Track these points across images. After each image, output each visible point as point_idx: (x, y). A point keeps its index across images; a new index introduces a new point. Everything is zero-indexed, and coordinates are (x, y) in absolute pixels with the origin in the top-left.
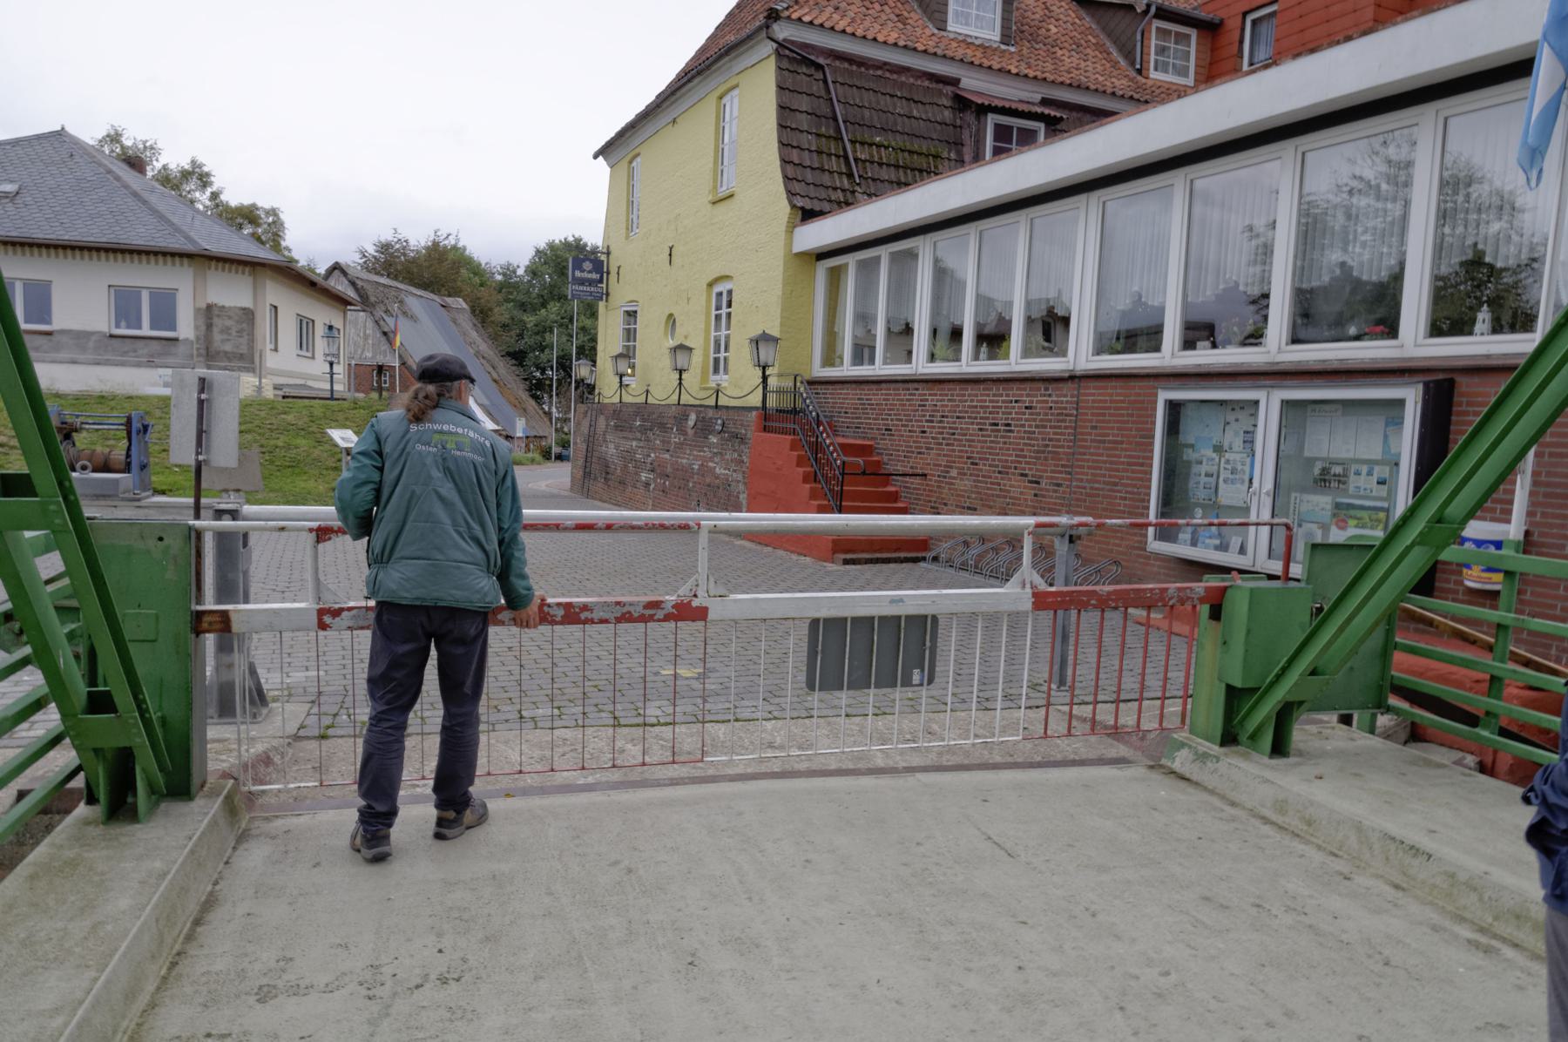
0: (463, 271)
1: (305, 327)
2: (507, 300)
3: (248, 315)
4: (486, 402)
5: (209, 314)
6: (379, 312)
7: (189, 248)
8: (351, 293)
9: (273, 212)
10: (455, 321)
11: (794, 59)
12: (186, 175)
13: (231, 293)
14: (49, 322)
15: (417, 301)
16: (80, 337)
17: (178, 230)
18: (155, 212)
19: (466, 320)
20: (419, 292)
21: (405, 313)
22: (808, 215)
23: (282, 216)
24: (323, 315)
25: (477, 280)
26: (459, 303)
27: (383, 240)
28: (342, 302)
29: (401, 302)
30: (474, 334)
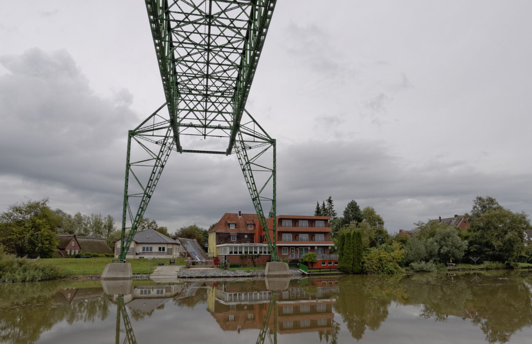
0: (196, 231)
1: (176, 248)
2: (204, 236)
3: (172, 249)
4: (199, 257)
5: (168, 249)
6: (183, 244)
7: (166, 242)
8: (179, 243)
9: (166, 228)
10: (194, 244)
11: (217, 233)
12: (152, 223)
13: (170, 247)
14: (152, 251)
15: (189, 241)
16: (155, 253)
17: (165, 240)
18: (163, 238)
19: (196, 243)
20: (189, 240)
21: (187, 244)
22: (217, 244)
23: (167, 228)
24: (177, 247)
25: (199, 232)
26: (195, 240)
27: (182, 227)
28: (179, 245)
29: (186, 242)
30: (197, 245)
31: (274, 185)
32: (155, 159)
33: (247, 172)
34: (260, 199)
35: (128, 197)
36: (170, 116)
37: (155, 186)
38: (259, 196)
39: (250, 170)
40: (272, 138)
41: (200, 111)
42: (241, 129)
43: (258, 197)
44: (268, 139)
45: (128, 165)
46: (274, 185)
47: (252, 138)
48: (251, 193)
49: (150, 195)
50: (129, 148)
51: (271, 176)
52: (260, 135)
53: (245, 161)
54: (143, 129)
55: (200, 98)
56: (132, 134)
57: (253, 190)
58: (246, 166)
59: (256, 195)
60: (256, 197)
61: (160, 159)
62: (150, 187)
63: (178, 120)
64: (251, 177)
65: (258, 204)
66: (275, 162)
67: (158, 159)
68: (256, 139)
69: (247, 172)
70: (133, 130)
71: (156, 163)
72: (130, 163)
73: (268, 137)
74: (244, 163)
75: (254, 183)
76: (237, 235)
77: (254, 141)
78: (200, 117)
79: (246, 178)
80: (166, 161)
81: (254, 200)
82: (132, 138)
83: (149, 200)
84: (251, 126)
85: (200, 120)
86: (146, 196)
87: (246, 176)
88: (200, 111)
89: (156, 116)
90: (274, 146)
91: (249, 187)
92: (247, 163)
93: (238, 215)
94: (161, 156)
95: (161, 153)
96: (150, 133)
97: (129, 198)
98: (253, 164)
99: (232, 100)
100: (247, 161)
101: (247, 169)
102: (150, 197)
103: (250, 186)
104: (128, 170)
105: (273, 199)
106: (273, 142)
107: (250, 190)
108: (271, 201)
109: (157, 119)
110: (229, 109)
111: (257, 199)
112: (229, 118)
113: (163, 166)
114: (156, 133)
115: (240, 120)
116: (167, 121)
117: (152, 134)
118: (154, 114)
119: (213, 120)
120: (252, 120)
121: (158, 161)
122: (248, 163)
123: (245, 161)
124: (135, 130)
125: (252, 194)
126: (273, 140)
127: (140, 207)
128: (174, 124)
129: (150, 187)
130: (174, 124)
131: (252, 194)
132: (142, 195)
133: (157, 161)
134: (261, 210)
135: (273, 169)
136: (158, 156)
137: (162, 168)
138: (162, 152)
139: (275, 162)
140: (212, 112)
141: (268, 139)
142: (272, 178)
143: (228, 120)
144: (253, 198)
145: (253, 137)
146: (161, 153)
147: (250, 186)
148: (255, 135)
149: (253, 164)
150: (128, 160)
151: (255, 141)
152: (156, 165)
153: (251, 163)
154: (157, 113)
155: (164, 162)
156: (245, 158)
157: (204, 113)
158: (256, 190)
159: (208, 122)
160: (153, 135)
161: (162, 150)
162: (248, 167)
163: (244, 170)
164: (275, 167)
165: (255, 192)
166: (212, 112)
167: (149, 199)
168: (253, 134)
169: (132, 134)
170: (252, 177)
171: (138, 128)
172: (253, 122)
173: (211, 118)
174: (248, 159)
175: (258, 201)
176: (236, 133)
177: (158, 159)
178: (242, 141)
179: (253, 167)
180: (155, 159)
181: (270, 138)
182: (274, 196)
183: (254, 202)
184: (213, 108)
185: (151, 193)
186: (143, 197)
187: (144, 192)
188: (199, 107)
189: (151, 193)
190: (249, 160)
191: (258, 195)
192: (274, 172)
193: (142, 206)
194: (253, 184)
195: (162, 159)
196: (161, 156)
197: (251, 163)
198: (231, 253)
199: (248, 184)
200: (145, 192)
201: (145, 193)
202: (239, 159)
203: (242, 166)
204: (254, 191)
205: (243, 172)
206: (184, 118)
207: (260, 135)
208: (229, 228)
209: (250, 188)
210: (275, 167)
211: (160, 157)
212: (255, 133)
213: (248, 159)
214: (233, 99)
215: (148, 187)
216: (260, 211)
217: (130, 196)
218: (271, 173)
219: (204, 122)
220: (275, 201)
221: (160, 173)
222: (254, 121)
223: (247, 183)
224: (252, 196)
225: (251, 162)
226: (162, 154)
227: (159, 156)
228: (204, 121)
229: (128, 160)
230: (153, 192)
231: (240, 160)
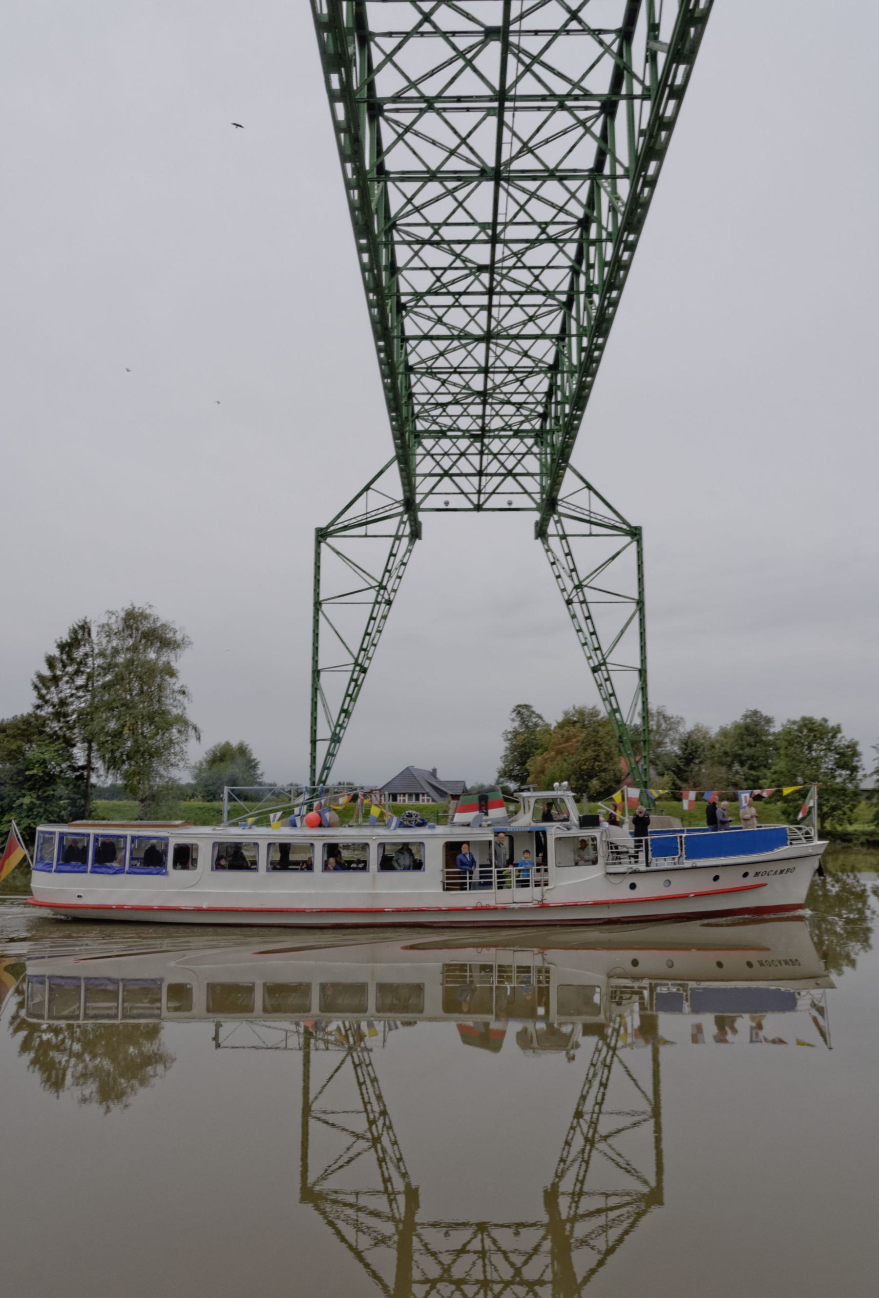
31: (642, 634)
32: (372, 587)
33: (576, 607)
34: (610, 667)
36: (405, 491)
37: (375, 645)
38: (608, 660)
39: (584, 602)
40: (634, 524)
41: (466, 475)
42: (560, 509)
43: (604, 664)
44: (624, 527)
45: (318, 604)
46: (642, 634)
47: (585, 528)
48: (589, 655)
49: (366, 666)
50: (317, 568)
52: (606, 520)
53: (573, 580)
54: (346, 524)
55: (463, 443)
56: (322, 535)
57: (592, 648)
58: (574, 593)
59: (600, 657)
60: (600, 665)
61: (385, 588)
62: (365, 650)
63: (418, 499)
64: (587, 618)
65: (606, 680)
66: (641, 580)
67: (381, 587)
68: (596, 530)
69: (576, 607)
70: (324, 525)
71: (377, 597)
72: (321, 598)
73: (624, 522)
74: (570, 586)
75: (594, 633)
77: (591, 535)
78: (467, 488)
79: (575, 620)
80: (395, 591)
81: (595, 670)
82: (323, 545)
83: (364, 678)
84: (583, 499)
85: (465, 494)
86: (358, 668)
87: (574, 617)
88: (466, 475)
89: (370, 491)
90: (639, 542)
91: (583, 641)
92: (576, 587)
94: (388, 581)
95: (387, 574)
96: (361, 531)
97: (322, 674)
98: (591, 588)
99: (536, 443)
101: (576, 599)
102: (364, 670)
103: (586, 639)
104: (318, 615)
105: (639, 666)
106: (635, 533)
107: (585, 647)
108: (636, 673)
109: (373, 502)
110: (532, 464)
111: (603, 668)
112: (533, 485)
113: (389, 603)
114: (372, 529)
115: (558, 490)
116: (397, 502)
117: (364, 534)
118: (367, 488)
119: (493, 493)
120: (584, 485)
121: (382, 592)
122: (579, 587)
123: (573, 580)
124: (328, 527)
125: (590, 658)
126: (636, 528)
127: (347, 695)
128: (410, 505)
129: (365, 650)
130: (410, 505)
131: (590, 658)
132: (351, 667)
133: (378, 591)
134: (613, 695)
135: (636, 597)
136: (380, 580)
137: (388, 607)
138: (389, 571)
139: (641, 580)
140: (492, 475)
141: (624, 527)
142: (636, 619)
143: (529, 490)
144: (592, 665)
145: (588, 525)
146: (387, 574)
147: (586, 639)
148: (592, 520)
149: (591, 588)
150: (317, 594)
151: (594, 533)
152: (377, 602)
153: (586, 586)
154: (372, 486)
155: (393, 594)
156: (571, 576)
157: (477, 478)
158: (599, 648)
159: (483, 498)
160: (366, 536)
161: (389, 568)
162: (580, 594)
163: (569, 602)
164: (641, 593)
165: (598, 652)
166: (492, 475)
167: (362, 675)
168: (588, 518)
170: (589, 618)
171: (332, 524)
172: (586, 490)
173: (489, 489)
174: (578, 576)
175: (605, 673)
176: (549, 520)
177: (381, 587)
178: (564, 537)
179: (590, 594)
180: (373, 587)
181: (629, 525)
182: (642, 661)
183: (596, 674)
184: (494, 467)
185: (368, 661)
186: (353, 671)
187: (353, 661)
188: (464, 466)
190: (581, 579)
191: (604, 659)
192: (640, 603)
193: (350, 692)
194: (592, 634)
195: (389, 588)
196: (388, 581)
197: (586, 586)
199: (580, 633)
200: (357, 660)
201: (356, 664)
202: (558, 577)
203: (565, 593)
204: (595, 649)
205: (569, 609)
206: (431, 492)
207: (606, 520)
209: (585, 644)
210: (641, 593)
211: (384, 584)
212: (592, 515)
213: (578, 576)
214: (539, 440)
215: (362, 649)
216: (611, 695)
217: (324, 669)
218: (633, 607)
219: (474, 498)
220: (645, 671)
221: (384, 617)
222: (589, 487)
223: (578, 631)
224: (591, 661)
225: (584, 583)
226: (390, 577)
227: (382, 580)
228: (476, 496)
229: (317, 594)
230: (370, 659)
231: (559, 580)
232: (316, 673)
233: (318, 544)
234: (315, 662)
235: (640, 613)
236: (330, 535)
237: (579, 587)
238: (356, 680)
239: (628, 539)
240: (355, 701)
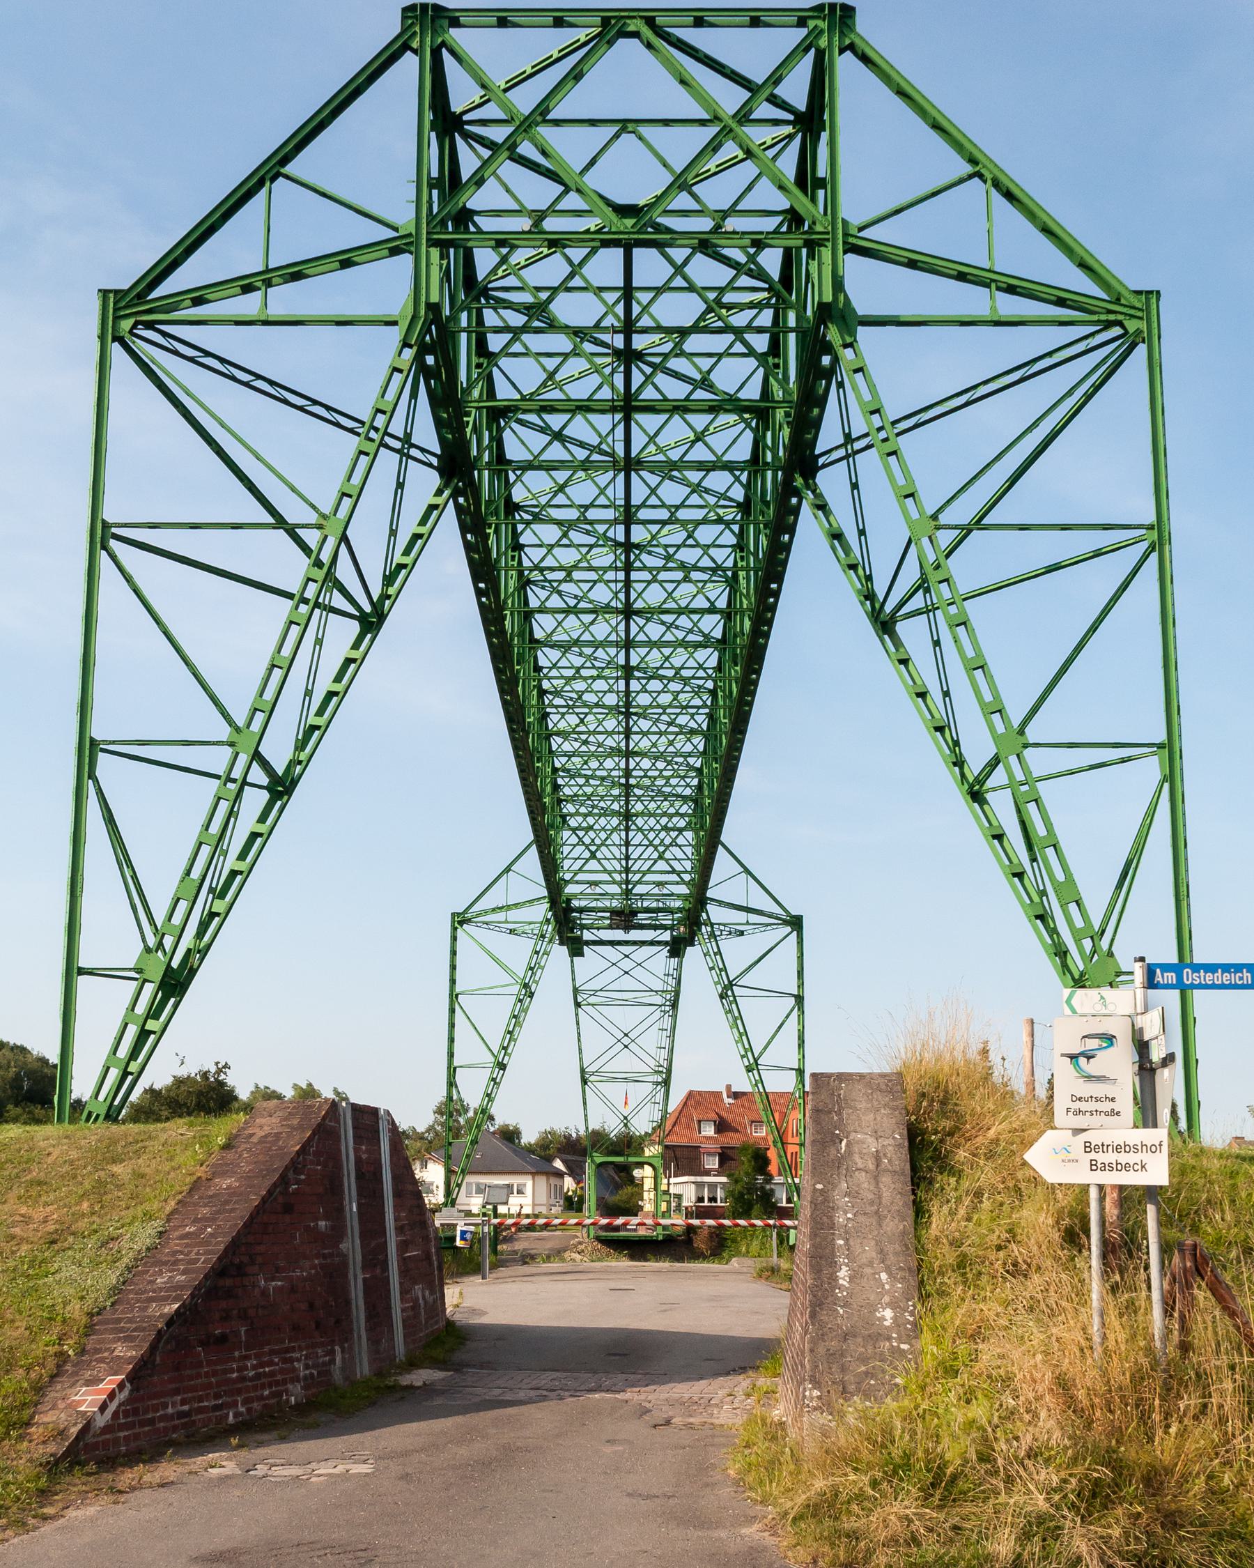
35: (455, 1069)
38: (759, 1062)
51: (792, 1010)
56: (460, 920)
66: (800, 974)
76: (720, 1151)
81: (749, 1069)
93: (725, 1095)
100: (726, 983)
102: (502, 1066)
106: (796, 923)
113: (531, 995)
118: (508, 870)
139: (800, 974)
144: (747, 1064)
163: (721, 997)
167: (501, 1072)
169: (460, 920)
177: (526, 986)
189: (507, 1058)
191: (756, 1060)
192: (799, 999)
198: (701, 1199)
208: (700, 1133)
224: (745, 1059)
230: (510, 1055)
232: (452, 1071)
233: (455, 929)
234: (451, 1055)
235: (799, 1010)
236: (468, 921)
237: (731, 985)
238: (495, 1083)
239: (789, 929)
240: (493, 1101)
